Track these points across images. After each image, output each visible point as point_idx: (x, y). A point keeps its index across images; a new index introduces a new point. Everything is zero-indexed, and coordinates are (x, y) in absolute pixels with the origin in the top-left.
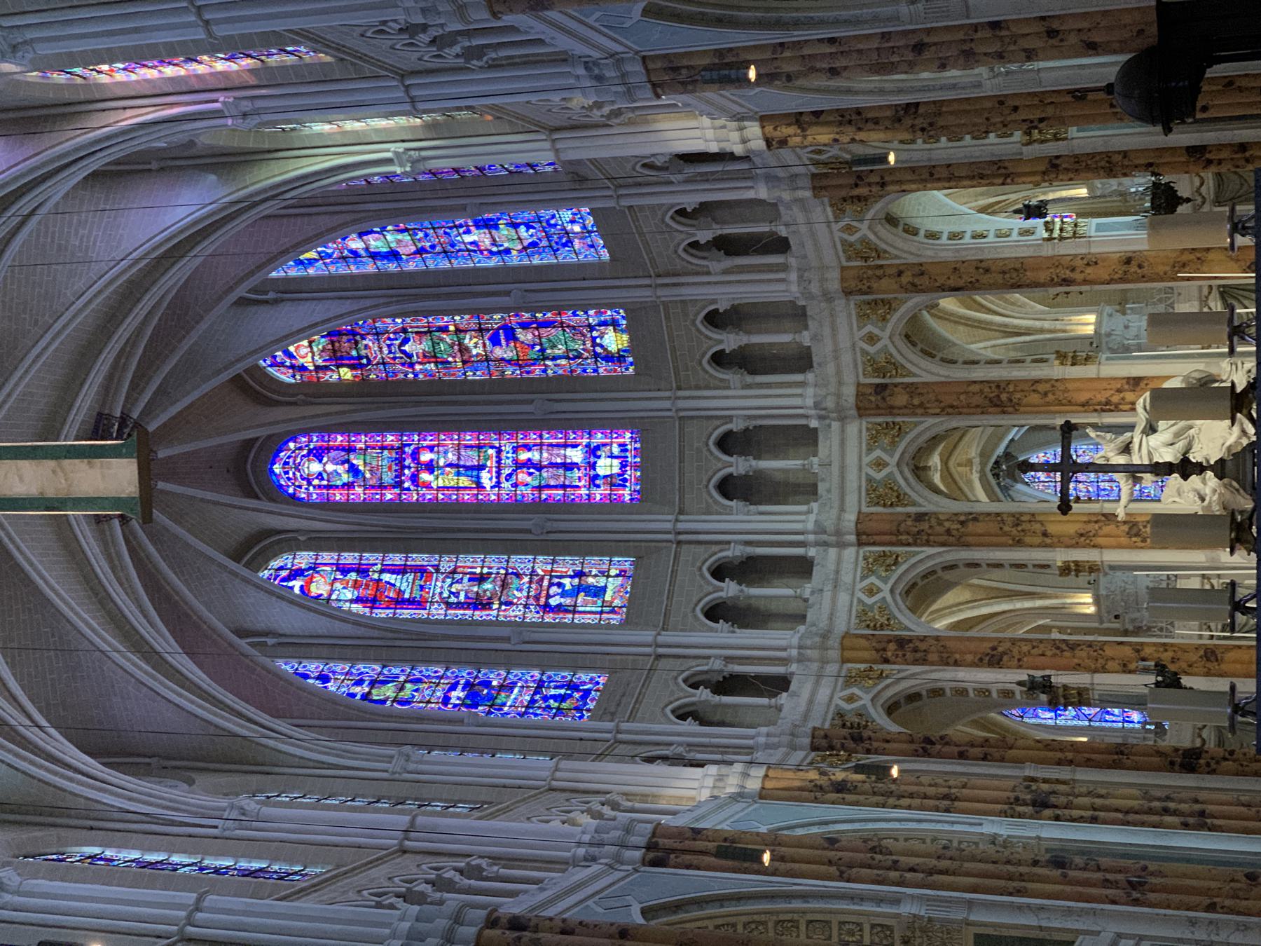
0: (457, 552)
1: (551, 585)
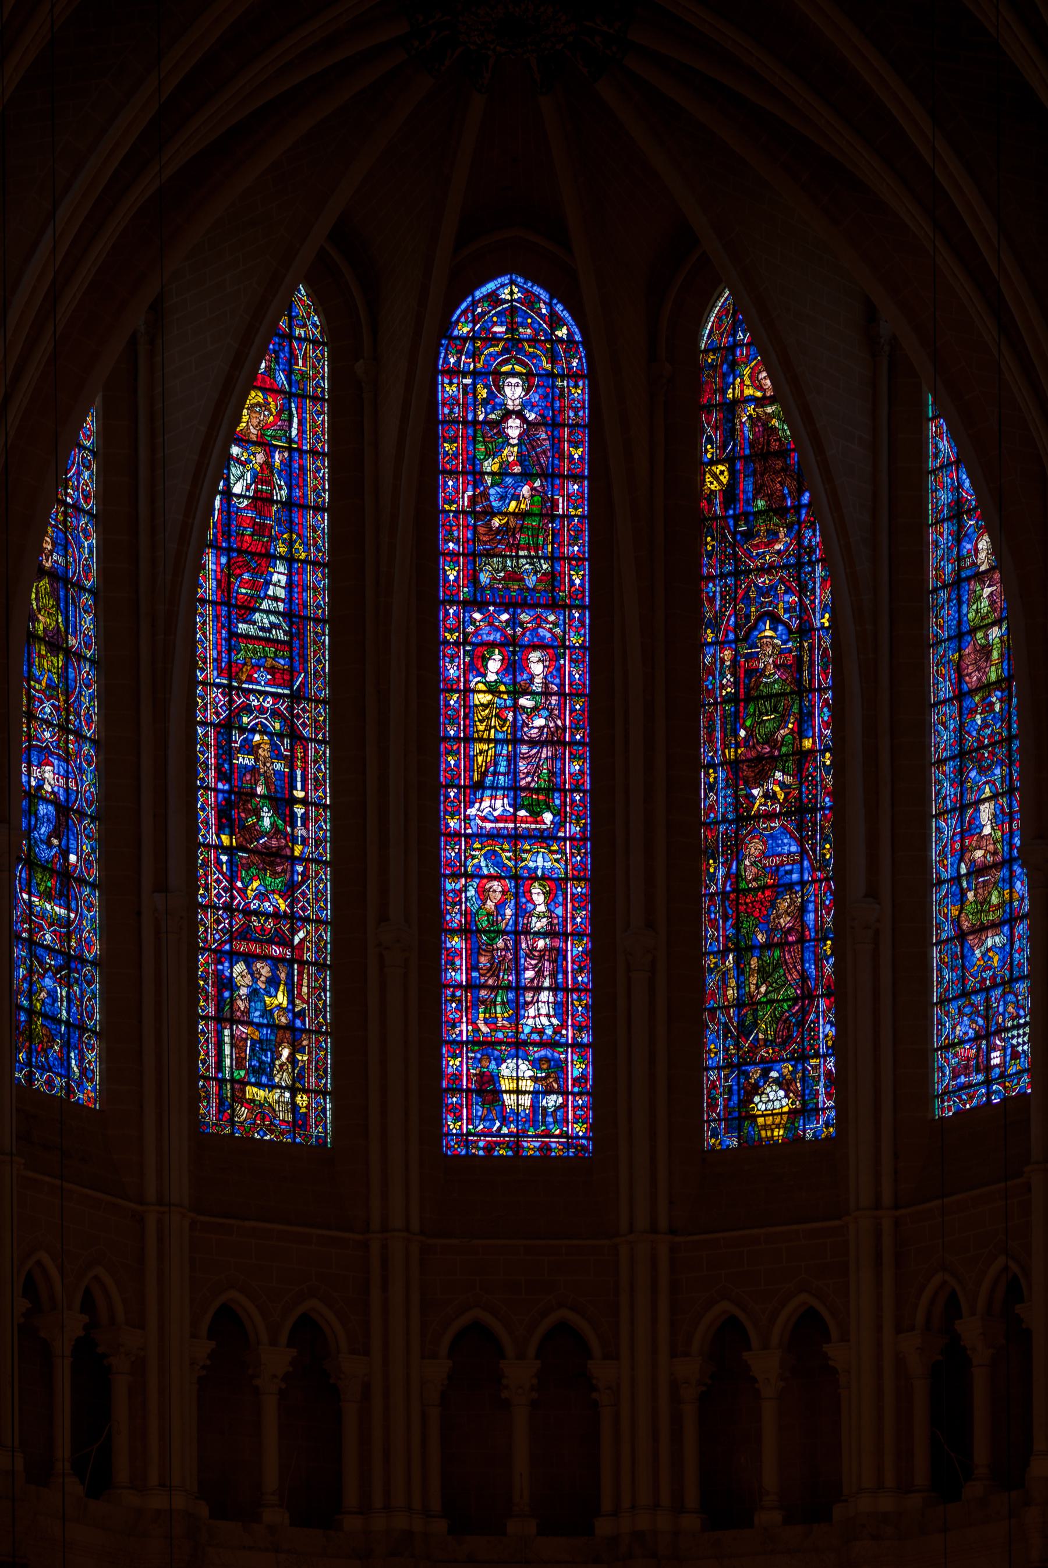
0: (333, 742)
1: (275, 962)
